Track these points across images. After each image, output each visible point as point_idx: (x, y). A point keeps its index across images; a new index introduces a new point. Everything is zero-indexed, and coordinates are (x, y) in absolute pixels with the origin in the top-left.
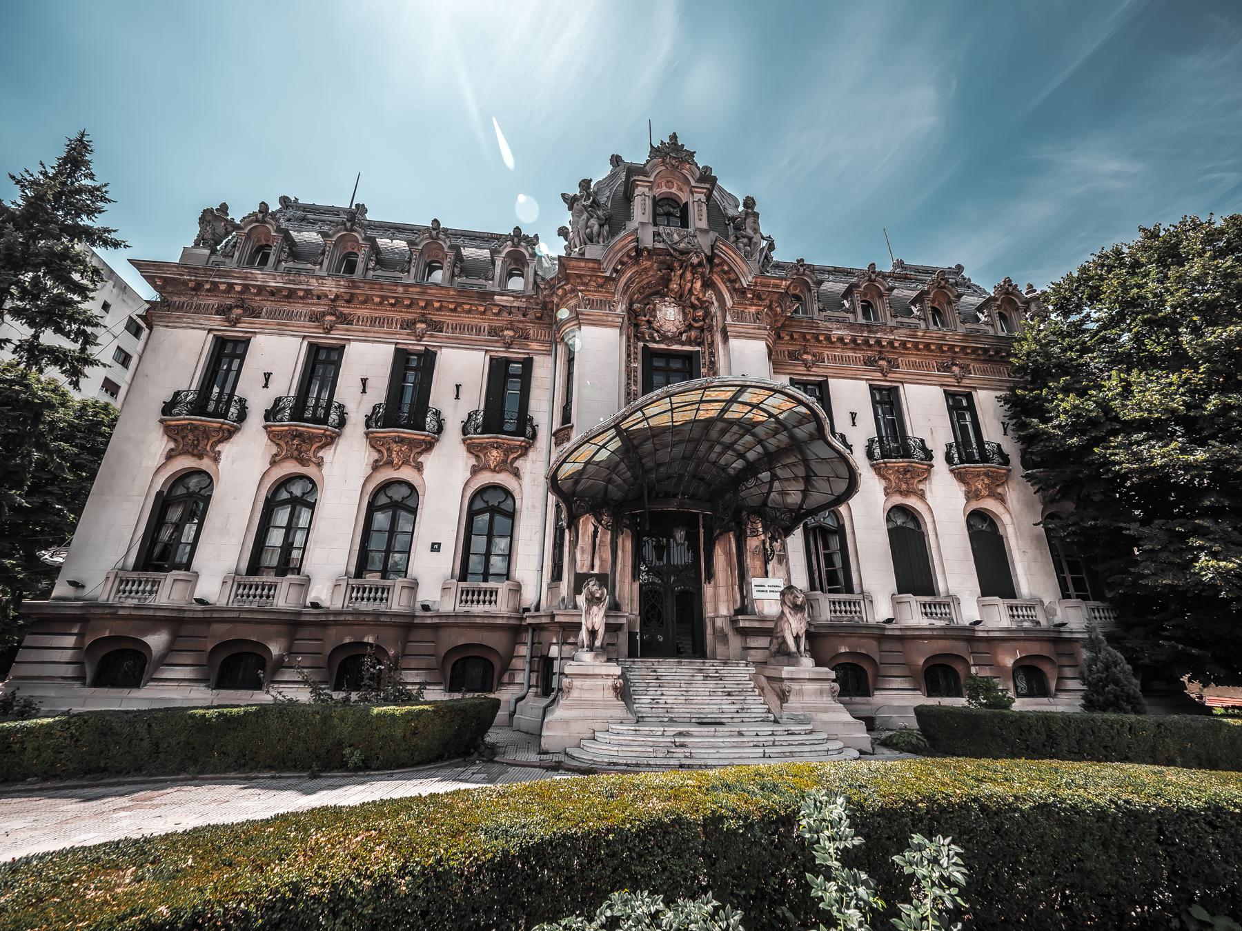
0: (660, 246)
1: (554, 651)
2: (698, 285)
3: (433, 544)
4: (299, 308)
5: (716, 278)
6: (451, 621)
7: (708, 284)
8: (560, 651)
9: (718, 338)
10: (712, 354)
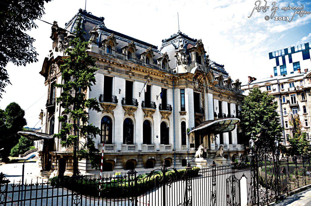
0: (200, 70)
1: (187, 158)
2: (202, 78)
3: (157, 136)
4: (123, 69)
5: (206, 77)
6: (165, 153)
7: (204, 79)
8: (188, 158)
9: (205, 91)
10: (203, 95)
